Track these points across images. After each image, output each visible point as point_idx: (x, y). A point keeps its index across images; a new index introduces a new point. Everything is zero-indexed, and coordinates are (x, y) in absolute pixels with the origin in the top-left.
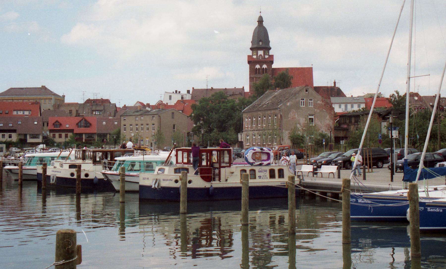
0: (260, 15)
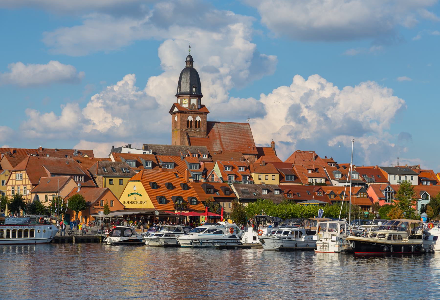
0: (189, 55)
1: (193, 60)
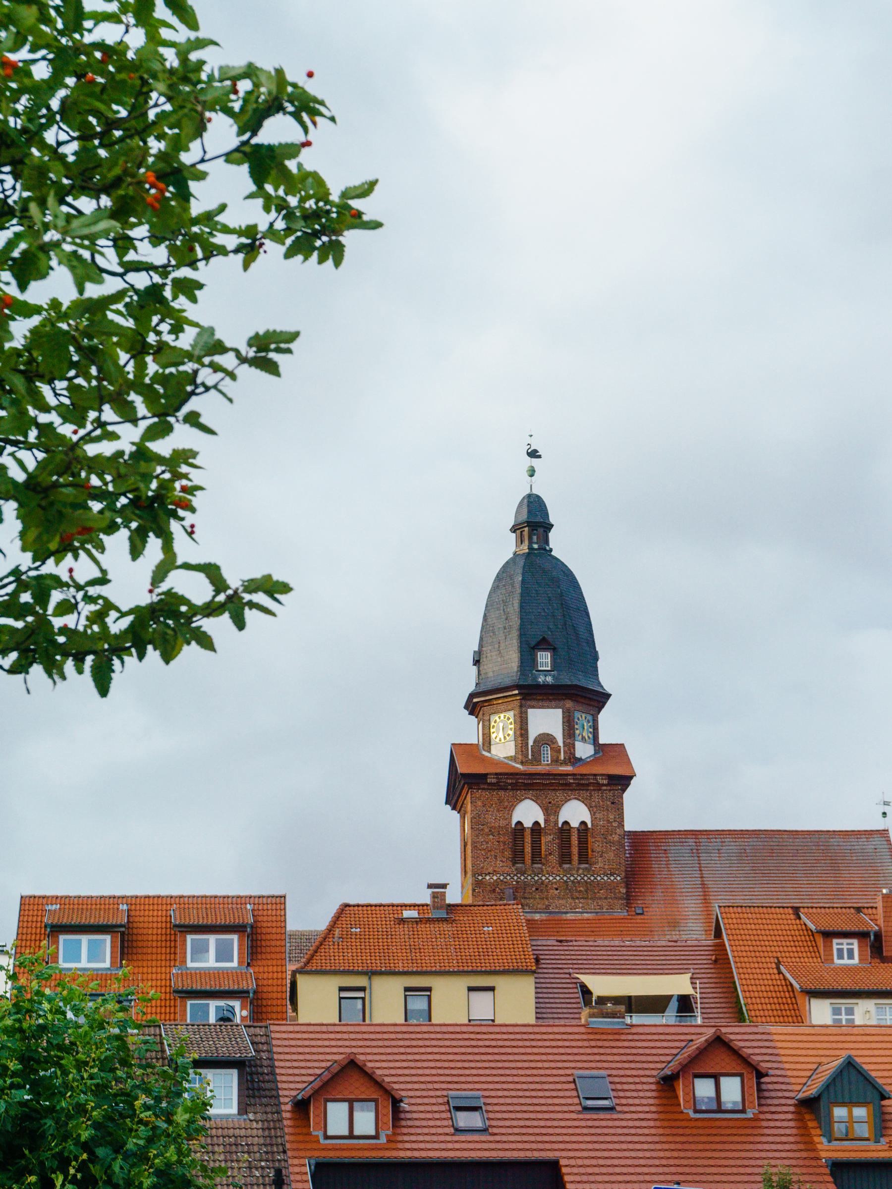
0: (528, 492)
1: (552, 520)
